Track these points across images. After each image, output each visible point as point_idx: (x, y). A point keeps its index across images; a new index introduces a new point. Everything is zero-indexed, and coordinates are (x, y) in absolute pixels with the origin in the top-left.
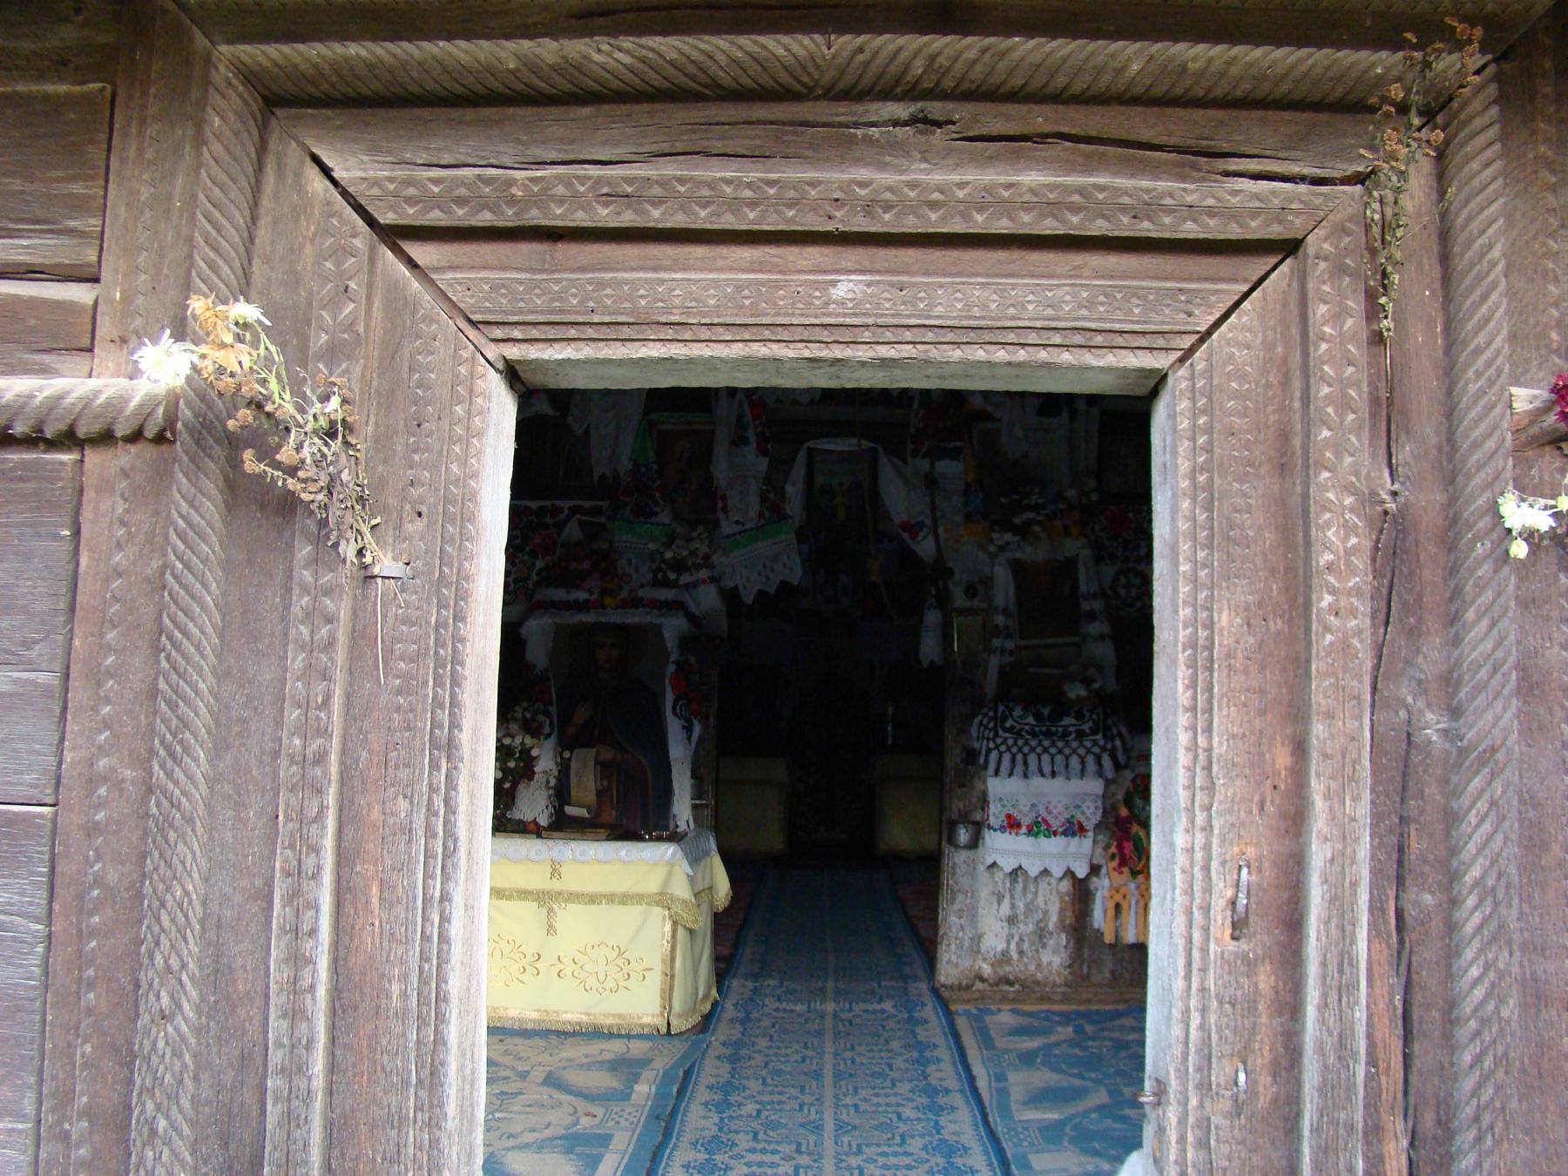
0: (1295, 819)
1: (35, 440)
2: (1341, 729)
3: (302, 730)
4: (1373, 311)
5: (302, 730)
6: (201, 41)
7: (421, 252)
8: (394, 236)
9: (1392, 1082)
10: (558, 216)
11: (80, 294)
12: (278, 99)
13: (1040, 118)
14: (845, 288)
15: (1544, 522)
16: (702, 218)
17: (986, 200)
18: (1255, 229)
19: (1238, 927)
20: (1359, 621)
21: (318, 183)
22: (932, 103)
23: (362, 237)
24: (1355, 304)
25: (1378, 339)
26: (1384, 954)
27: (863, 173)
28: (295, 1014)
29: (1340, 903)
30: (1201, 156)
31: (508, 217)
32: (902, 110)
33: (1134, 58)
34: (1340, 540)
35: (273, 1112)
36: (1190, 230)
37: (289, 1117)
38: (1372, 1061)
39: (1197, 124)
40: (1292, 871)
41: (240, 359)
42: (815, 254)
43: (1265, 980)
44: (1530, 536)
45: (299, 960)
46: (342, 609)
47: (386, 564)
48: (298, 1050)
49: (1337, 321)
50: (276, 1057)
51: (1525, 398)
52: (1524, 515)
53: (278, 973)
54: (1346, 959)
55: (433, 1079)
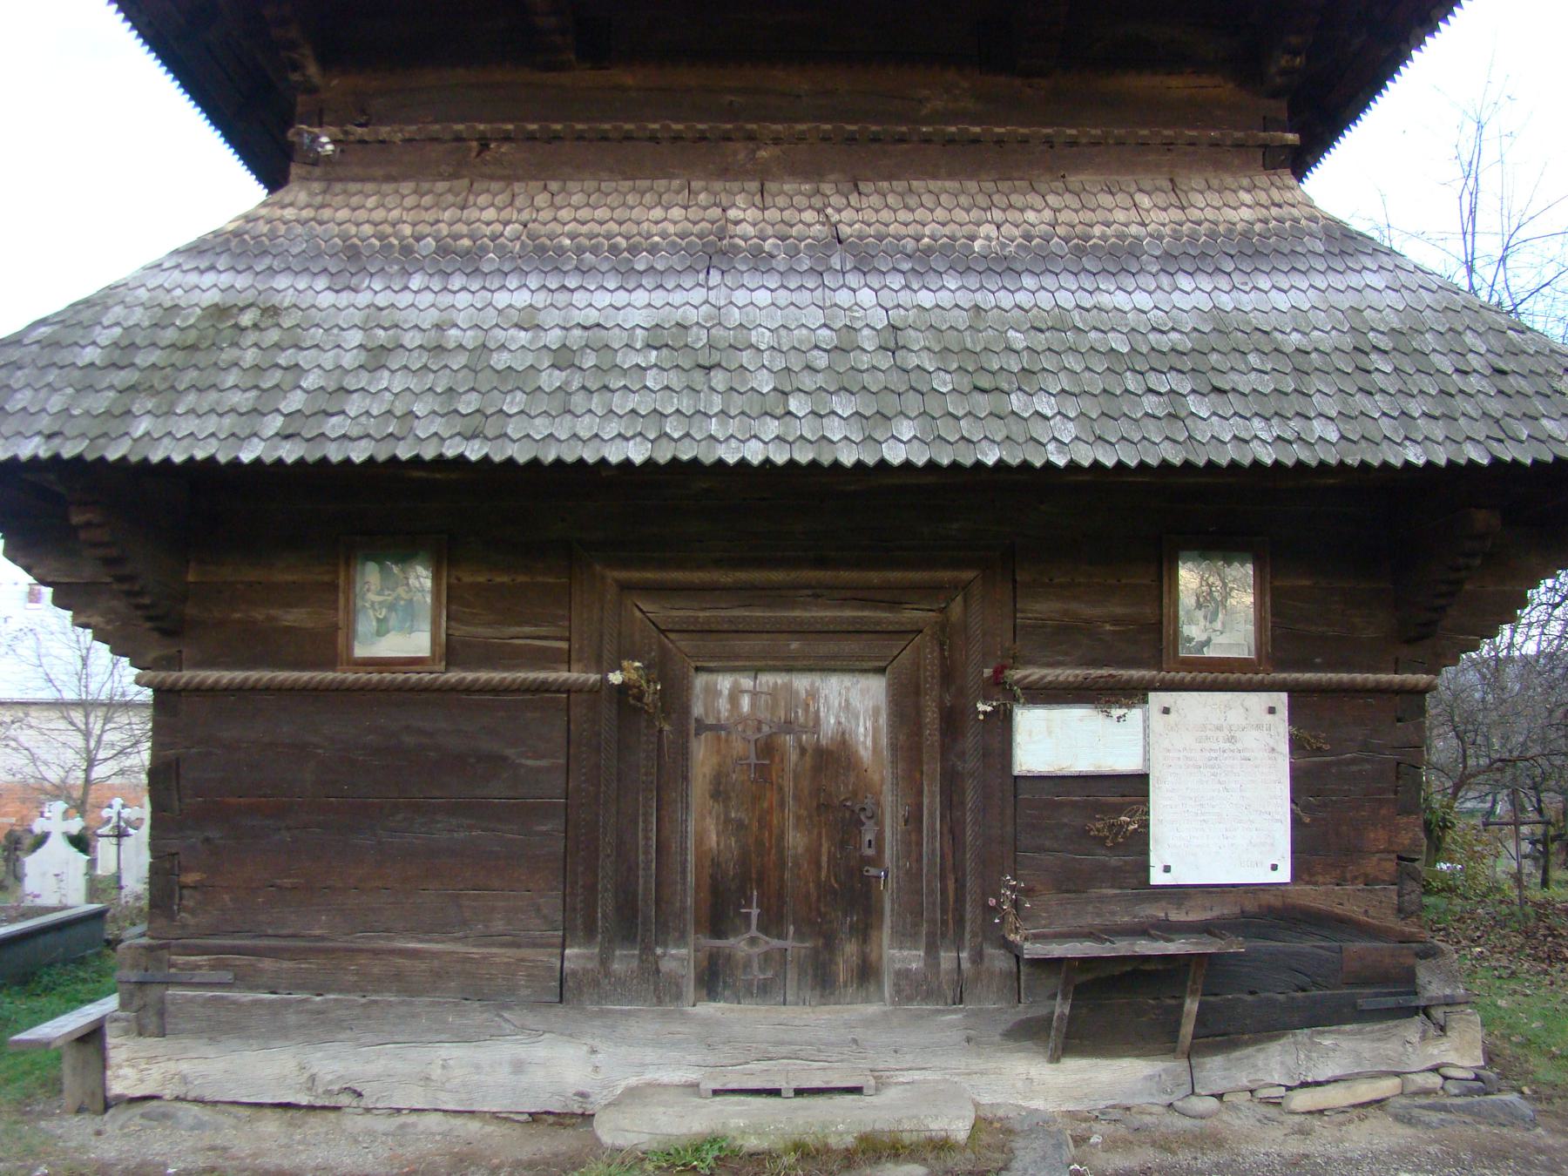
0: (920, 793)
1: (558, 691)
2: (932, 768)
3: (646, 774)
4: (942, 650)
5: (646, 774)
6: (598, 568)
7: (672, 636)
8: (663, 632)
9: (949, 863)
10: (714, 627)
11: (564, 645)
12: (626, 587)
13: (849, 594)
14: (794, 645)
15: (989, 709)
16: (754, 627)
17: (833, 620)
18: (909, 627)
19: (906, 822)
20: (937, 737)
21: (638, 614)
22: (818, 593)
23: (655, 632)
24: (937, 649)
25: (943, 658)
26: (946, 830)
27: (797, 613)
28: (647, 853)
29: (932, 815)
30: (895, 605)
31: (699, 627)
32: (809, 592)
33: (875, 577)
34: (931, 715)
35: (641, 881)
36: (891, 628)
37: (645, 882)
38: (942, 857)
39: (893, 598)
40: (920, 806)
41: (634, 676)
42: (785, 636)
43: (914, 837)
44: (985, 713)
45: (647, 839)
46: (654, 739)
47: (667, 727)
48: (648, 863)
49: (931, 656)
50: (641, 866)
51: (988, 672)
52: (981, 707)
53: (641, 843)
54: (934, 830)
55: (684, 872)
